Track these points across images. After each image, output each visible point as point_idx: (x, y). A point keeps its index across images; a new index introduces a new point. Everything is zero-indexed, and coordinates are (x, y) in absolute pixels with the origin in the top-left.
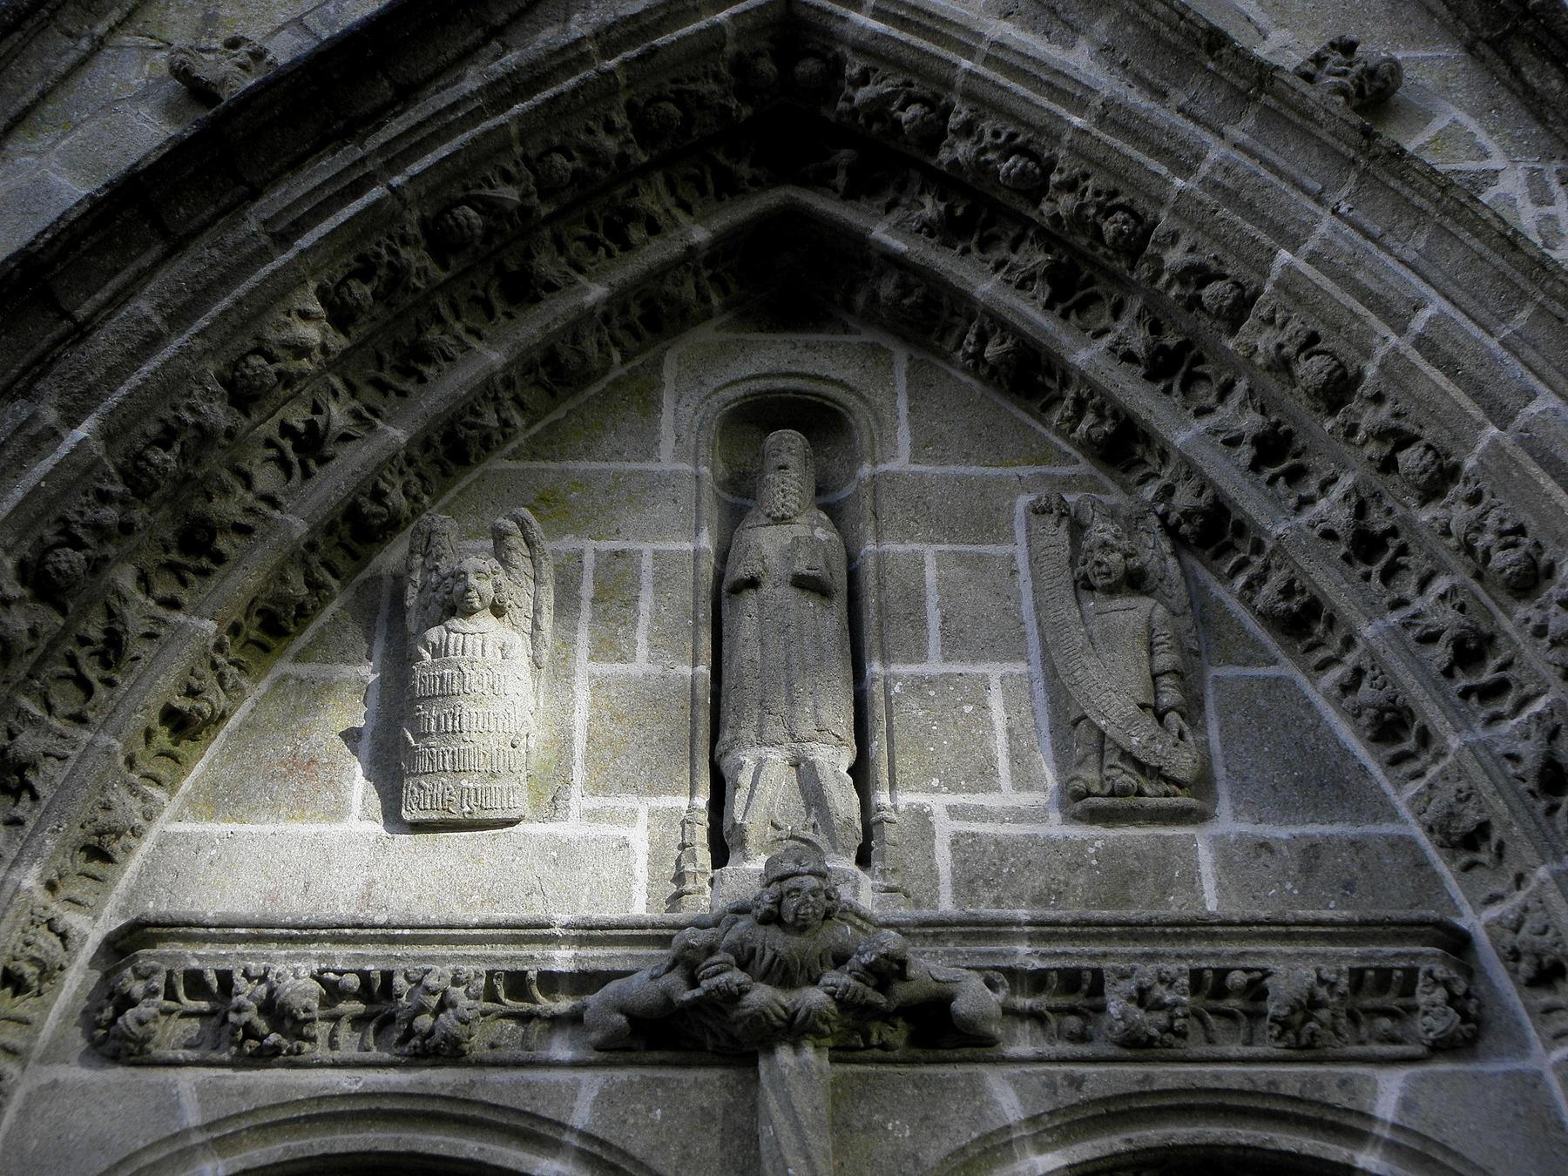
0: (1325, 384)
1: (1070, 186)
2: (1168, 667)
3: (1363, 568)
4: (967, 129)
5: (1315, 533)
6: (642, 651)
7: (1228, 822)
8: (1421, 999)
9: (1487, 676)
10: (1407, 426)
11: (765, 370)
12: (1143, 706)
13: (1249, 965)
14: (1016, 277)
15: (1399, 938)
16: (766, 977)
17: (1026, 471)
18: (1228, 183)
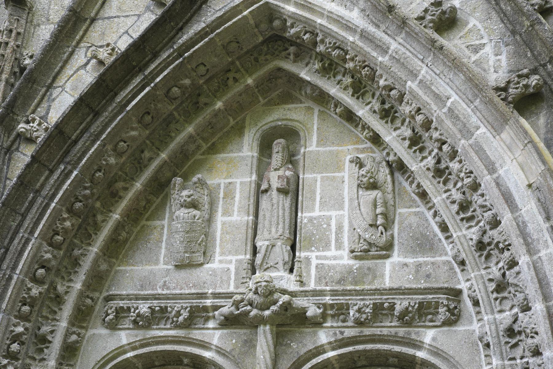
0: (423, 124)
1: (352, 59)
2: (380, 212)
3: (438, 180)
4: (322, 41)
5: (425, 169)
6: (236, 213)
7: (396, 258)
8: (440, 310)
9: (469, 214)
10: (443, 138)
11: (275, 119)
12: (371, 225)
13: (390, 301)
14: (343, 86)
15: (436, 293)
16: (256, 308)
17: (350, 147)
18: (397, 57)
